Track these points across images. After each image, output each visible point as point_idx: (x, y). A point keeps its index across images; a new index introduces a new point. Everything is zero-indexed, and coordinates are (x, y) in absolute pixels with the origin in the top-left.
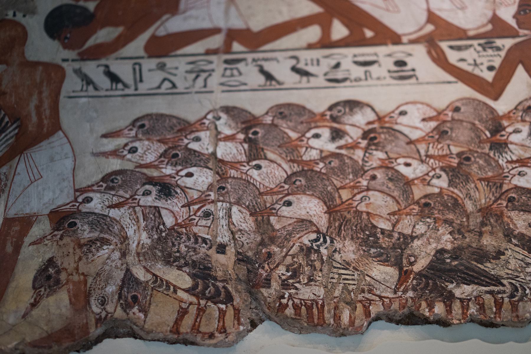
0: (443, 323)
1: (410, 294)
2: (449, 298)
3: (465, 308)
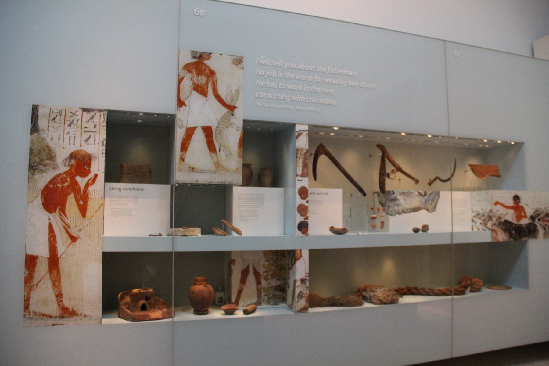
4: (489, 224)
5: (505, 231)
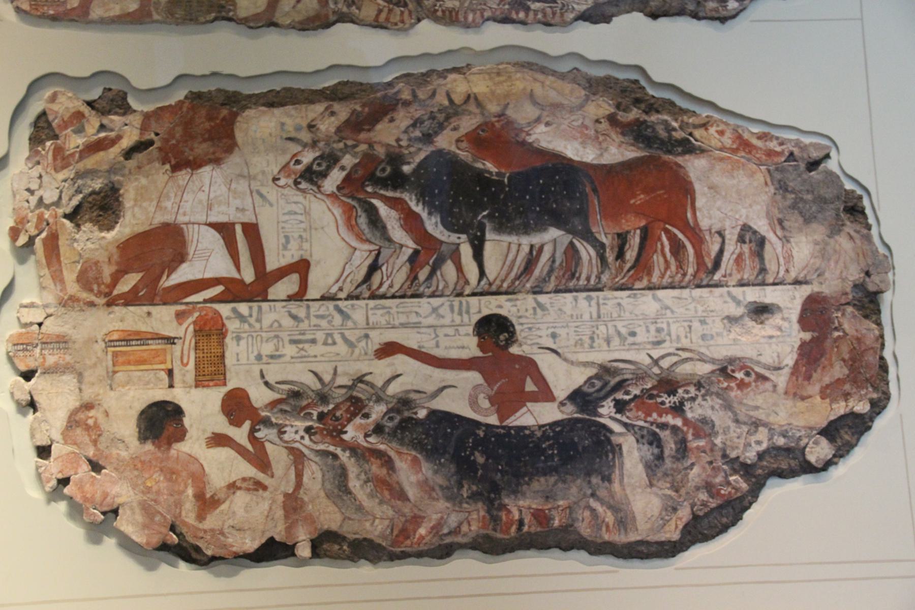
0: (523, 23)
1: (507, 7)
2: (527, 9)
3: (536, 15)
4: (352, 433)
5: (433, 453)
